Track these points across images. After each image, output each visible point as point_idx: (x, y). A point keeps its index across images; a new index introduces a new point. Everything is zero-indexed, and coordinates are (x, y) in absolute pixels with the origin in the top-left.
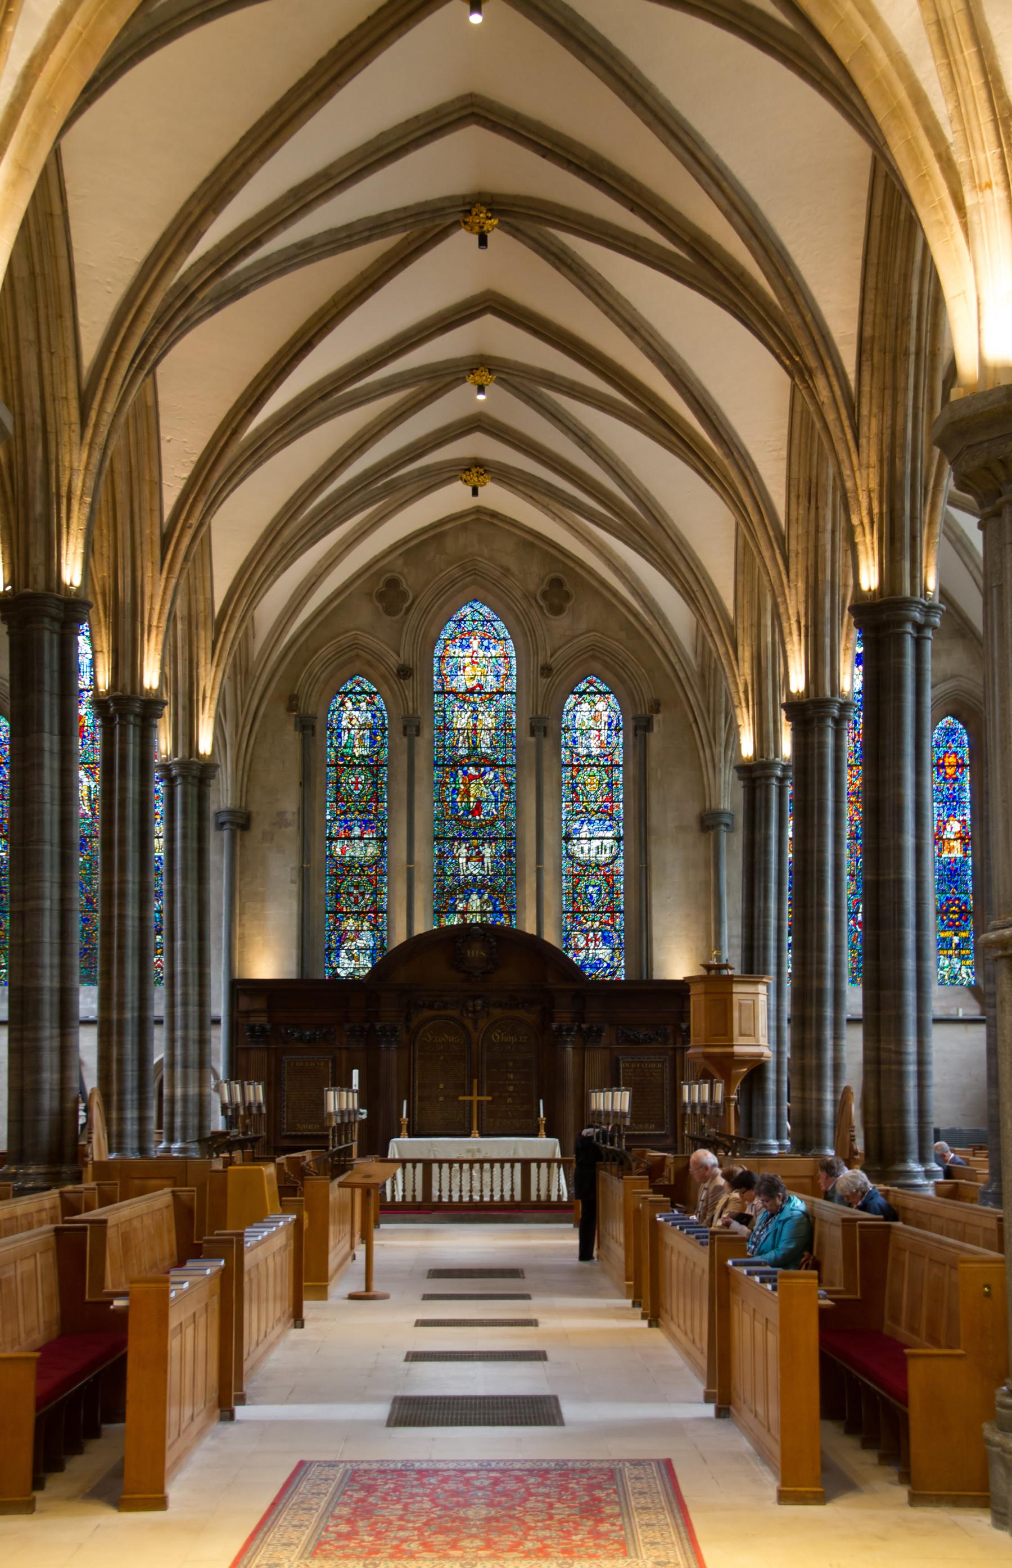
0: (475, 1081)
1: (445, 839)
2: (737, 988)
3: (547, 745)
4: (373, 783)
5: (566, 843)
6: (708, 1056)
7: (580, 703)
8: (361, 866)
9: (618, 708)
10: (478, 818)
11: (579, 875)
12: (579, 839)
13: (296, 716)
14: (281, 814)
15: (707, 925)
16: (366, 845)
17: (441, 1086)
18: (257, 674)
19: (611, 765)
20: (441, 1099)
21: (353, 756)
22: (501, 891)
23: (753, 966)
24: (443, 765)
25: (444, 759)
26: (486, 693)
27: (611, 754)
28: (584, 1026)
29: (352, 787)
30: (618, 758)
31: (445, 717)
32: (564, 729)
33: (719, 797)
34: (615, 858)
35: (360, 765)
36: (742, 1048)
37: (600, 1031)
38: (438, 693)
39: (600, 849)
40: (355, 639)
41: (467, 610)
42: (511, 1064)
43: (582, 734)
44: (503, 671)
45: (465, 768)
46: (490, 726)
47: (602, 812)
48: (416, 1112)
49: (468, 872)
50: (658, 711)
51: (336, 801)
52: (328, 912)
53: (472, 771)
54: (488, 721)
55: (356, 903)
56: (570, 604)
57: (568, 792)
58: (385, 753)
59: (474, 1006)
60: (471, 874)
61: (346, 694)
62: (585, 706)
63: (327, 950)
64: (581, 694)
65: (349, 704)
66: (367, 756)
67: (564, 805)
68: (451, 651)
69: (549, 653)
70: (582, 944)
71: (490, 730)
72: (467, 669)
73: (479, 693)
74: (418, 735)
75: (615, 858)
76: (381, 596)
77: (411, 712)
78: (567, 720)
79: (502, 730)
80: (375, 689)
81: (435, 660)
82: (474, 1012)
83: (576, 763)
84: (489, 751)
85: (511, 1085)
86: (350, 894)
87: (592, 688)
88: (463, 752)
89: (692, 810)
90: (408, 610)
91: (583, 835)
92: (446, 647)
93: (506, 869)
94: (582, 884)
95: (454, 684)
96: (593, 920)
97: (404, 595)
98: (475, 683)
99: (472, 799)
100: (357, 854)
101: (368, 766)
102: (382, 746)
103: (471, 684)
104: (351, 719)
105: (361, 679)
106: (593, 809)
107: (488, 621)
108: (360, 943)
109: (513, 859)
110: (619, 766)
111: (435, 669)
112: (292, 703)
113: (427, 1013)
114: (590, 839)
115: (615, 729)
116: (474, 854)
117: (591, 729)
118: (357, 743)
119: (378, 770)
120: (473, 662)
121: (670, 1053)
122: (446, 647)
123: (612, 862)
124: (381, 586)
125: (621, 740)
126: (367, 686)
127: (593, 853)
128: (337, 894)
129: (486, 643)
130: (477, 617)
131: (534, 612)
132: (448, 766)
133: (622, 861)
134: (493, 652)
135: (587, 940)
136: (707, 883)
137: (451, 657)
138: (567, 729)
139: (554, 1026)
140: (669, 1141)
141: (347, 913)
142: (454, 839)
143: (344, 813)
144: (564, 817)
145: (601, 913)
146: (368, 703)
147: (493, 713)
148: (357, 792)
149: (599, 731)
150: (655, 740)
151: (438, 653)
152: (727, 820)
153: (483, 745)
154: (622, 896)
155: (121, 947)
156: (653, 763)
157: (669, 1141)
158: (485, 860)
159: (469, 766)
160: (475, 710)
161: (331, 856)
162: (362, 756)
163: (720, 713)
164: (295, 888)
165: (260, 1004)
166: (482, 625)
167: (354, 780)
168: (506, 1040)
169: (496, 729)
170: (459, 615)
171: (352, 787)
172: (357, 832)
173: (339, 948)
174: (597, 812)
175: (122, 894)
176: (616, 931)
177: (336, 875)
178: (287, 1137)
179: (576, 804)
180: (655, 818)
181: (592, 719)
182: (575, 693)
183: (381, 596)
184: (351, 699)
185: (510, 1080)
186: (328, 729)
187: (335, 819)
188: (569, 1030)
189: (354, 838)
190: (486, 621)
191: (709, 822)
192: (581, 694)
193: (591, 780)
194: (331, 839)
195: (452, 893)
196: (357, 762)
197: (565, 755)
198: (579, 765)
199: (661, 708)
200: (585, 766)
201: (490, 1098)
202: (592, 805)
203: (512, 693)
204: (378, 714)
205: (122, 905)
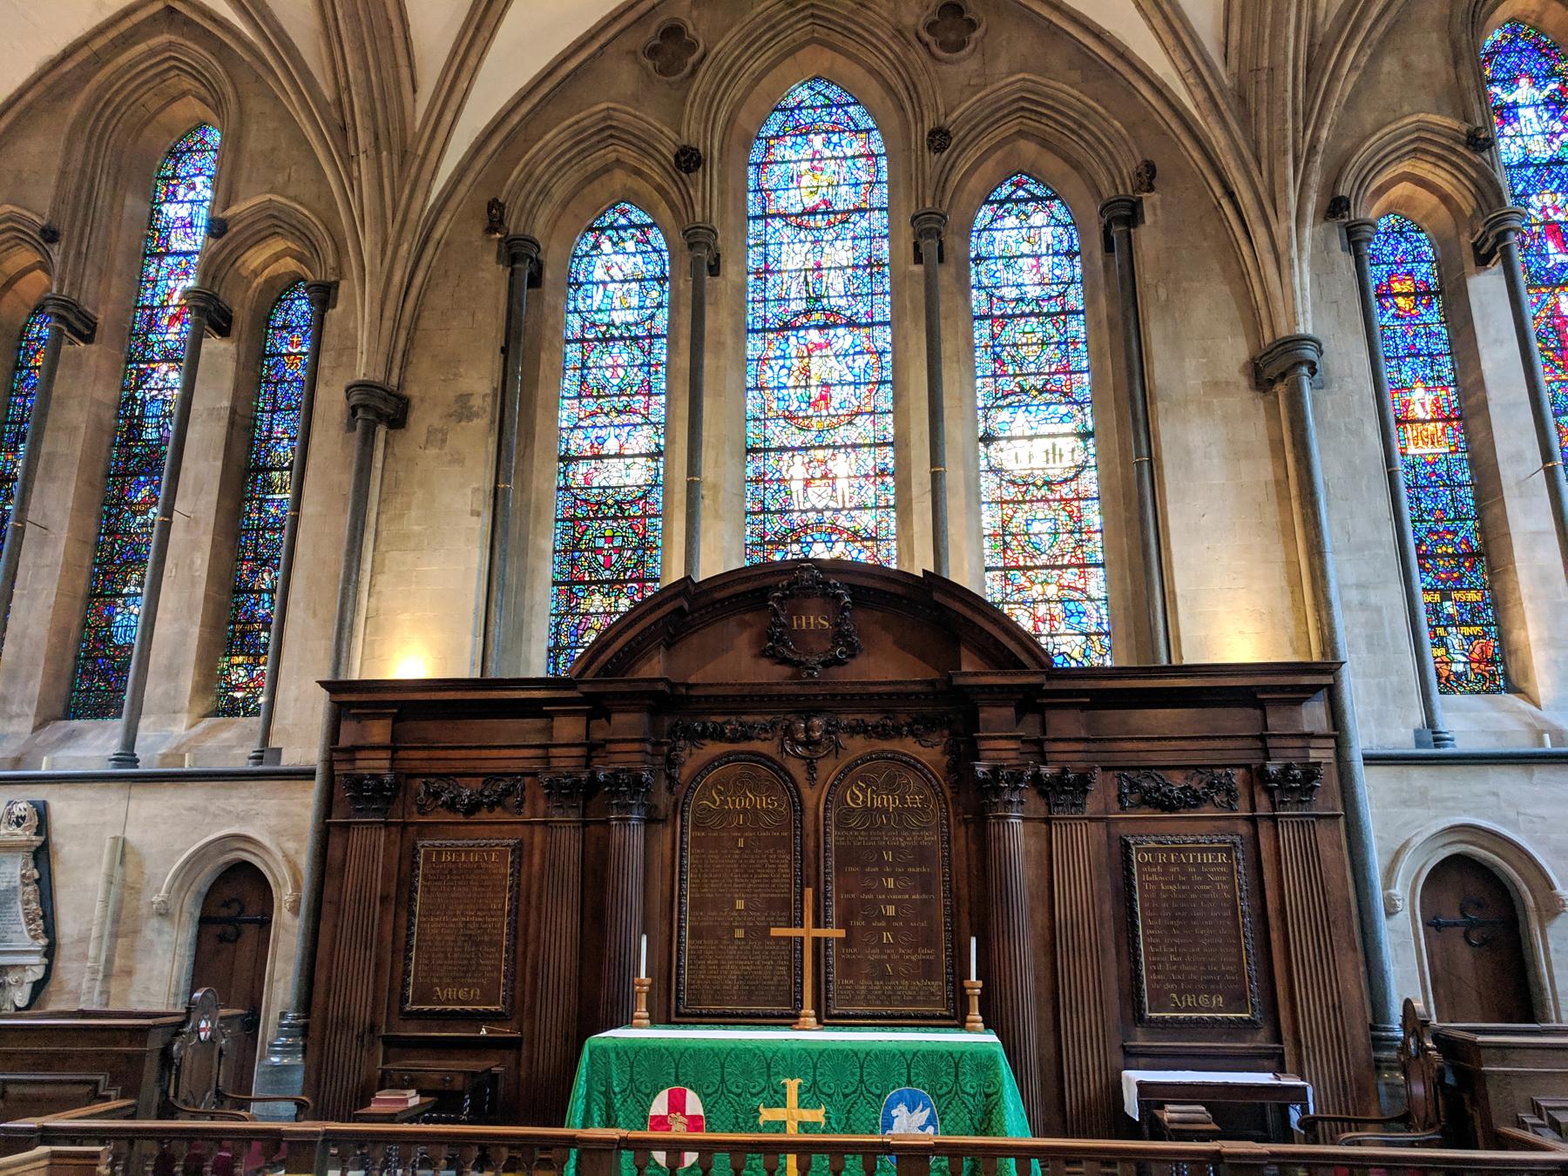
0: (809, 892)
1: (770, 450)
3: (945, 276)
4: (642, 365)
5: (987, 446)
7: (1002, 217)
8: (617, 502)
9: (1069, 220)
10: (824, 413)
11: (1013, 501)
12: (1010, 439)
13: (500, 240)
14: (464, 398)
15: (1291, 565)
16: (628, 467)
17: (740, 905)
18: (420, 152)
19: (1063, 312)
20: (740, 933)
21: (611, 324)
22: (866, 539)
24: (764, 330)
25: (765, 320)
26: (835, 213)
27: (1062, 294)
28: (1046, 771)
29: (608, 374)
30: (1075, 299)
31: (766, 256)
32: (974, 260)
33: (1294, 314)
34: (1082, 468)
35: (622, 338)
37: (1083, 781)
38: (755, 218)
39: (1054, 453)
40: (604, 119)
42: (888, 856)
43: (1007, 266)
45: (802, 333)
46: (845, 263)
47: (1051, 392)
48: (685, 961)
49: (808, 505)
50: (1151, 189)
51: (579, 396)
52: (555, 583)
53: (814, 336)
54: (840, 253)
55: (608, 565)
56: (977, 34)
57: (987, 358)
58: (662, 317)
59: (807, 730)
60: (814, 509)
61: (603, 230)
62: (1010, 221)
63: (549, 650)
64: (1002, 203)
65: (607, 247)
66: (636, 324)
67: (979, 382)
68: (780, 152)
69: (942, 111)
71: (842, 268)
72: (805, 181)
73: (823, 214)
74: (715, 270)
75: (1082, 468)
76: (653, 52)
77: (699, 219)
78: (978, 245)
79: (865, 267)
80: (649, 221)
81: (751, 170)
82: (809, 743)
83: (997, 313)
84: (843, 302)
85: (891, 902)
86: (599, 550)
87: (1021, 193)
89: (1235, 351)
90: (694, 72)
91: (1017, 432)
92: (768, 149)
93: (877, 497)
94: (1020, 518)
95: (783, 203)
96: (1045, 582)
97: (692, 46)
98: (817, 199)
99: (813, 382)
100: (613, 483)
101: (635, 339)
102: (660, 306)
103: (810, 202)
104: (608, 269)
105: (627, 206)
106: (1033, 387)
107: (839, 106)
109: (889, 480)
110: (1078, 313)
111: (751, 183)
112: (495, 215)
113: (714, 749)
114: (1030, 438)
115: (1067, 254)
116: (818, 475)
117: (1022, 256)
118: (617, 304)
119: (651, 344)
120: (814, 168)
121: (1244, 829)
122: (768, 149)
123: (1076, 476)
124: (650, 33)
125: (1078, 271)
126: (638, 216)
127: (1039, 461)
128: (572, 549)
129: (835, 138)
130: (820, 100)
131: (918, 57)
132: (770, 330)
133: (1094, 474)
134: (849, 152)
135: (1034, 617)
136: (1281, 484)
137: (776, 162)
138: (979, 259)
140: (1261, 1040)
141: (591, 583)
142: (782, 449)
143: (593, 414)
144: (980, 404)
145: (1061, 567)
146: (638, 242)
147: (849, 243)
148: (615, 381)
149: (1037, 257)
150: (1148, 239)
151: (755, 157)
152: (1311, 354)
153: (832, 293)
154: (1098, 536)
156: (1146, 275)
157: (1261, 1040)
158: (841, 484)
159: (807, 329)
160: (816, 242)
161: (567, 488)
162: (627, 325)
163: (1285, 153)
164: (482, 525)
165: (379, 731)
166: (830, 114)
167: (610, 361)
169: (855, 267)
171: (608, 374)
172: (611, 446)
174: (1041, 392)
176: (1089, 599)
177: (574, 519)
178: (418, 1015)
179: (1001, 380)
180: (1161, 369)
181: (1025, 248)
182: (992, 203)
183: (653, 52)
184: (610, 239)
186: (570, 285)
187: (576, 427)
188: (1015, 778)
189: (608, 456)
191: (1279, 368)
192: (1002, 203)
194: (567, 459)
196: (616, 334)
197: (978, 302)
198: (1003, 316)
199: (1155, 183)
200: (1013, 316)
201: (842, 933)
202: (1032, 380)
203: (881, 209)
204: (655, 256)
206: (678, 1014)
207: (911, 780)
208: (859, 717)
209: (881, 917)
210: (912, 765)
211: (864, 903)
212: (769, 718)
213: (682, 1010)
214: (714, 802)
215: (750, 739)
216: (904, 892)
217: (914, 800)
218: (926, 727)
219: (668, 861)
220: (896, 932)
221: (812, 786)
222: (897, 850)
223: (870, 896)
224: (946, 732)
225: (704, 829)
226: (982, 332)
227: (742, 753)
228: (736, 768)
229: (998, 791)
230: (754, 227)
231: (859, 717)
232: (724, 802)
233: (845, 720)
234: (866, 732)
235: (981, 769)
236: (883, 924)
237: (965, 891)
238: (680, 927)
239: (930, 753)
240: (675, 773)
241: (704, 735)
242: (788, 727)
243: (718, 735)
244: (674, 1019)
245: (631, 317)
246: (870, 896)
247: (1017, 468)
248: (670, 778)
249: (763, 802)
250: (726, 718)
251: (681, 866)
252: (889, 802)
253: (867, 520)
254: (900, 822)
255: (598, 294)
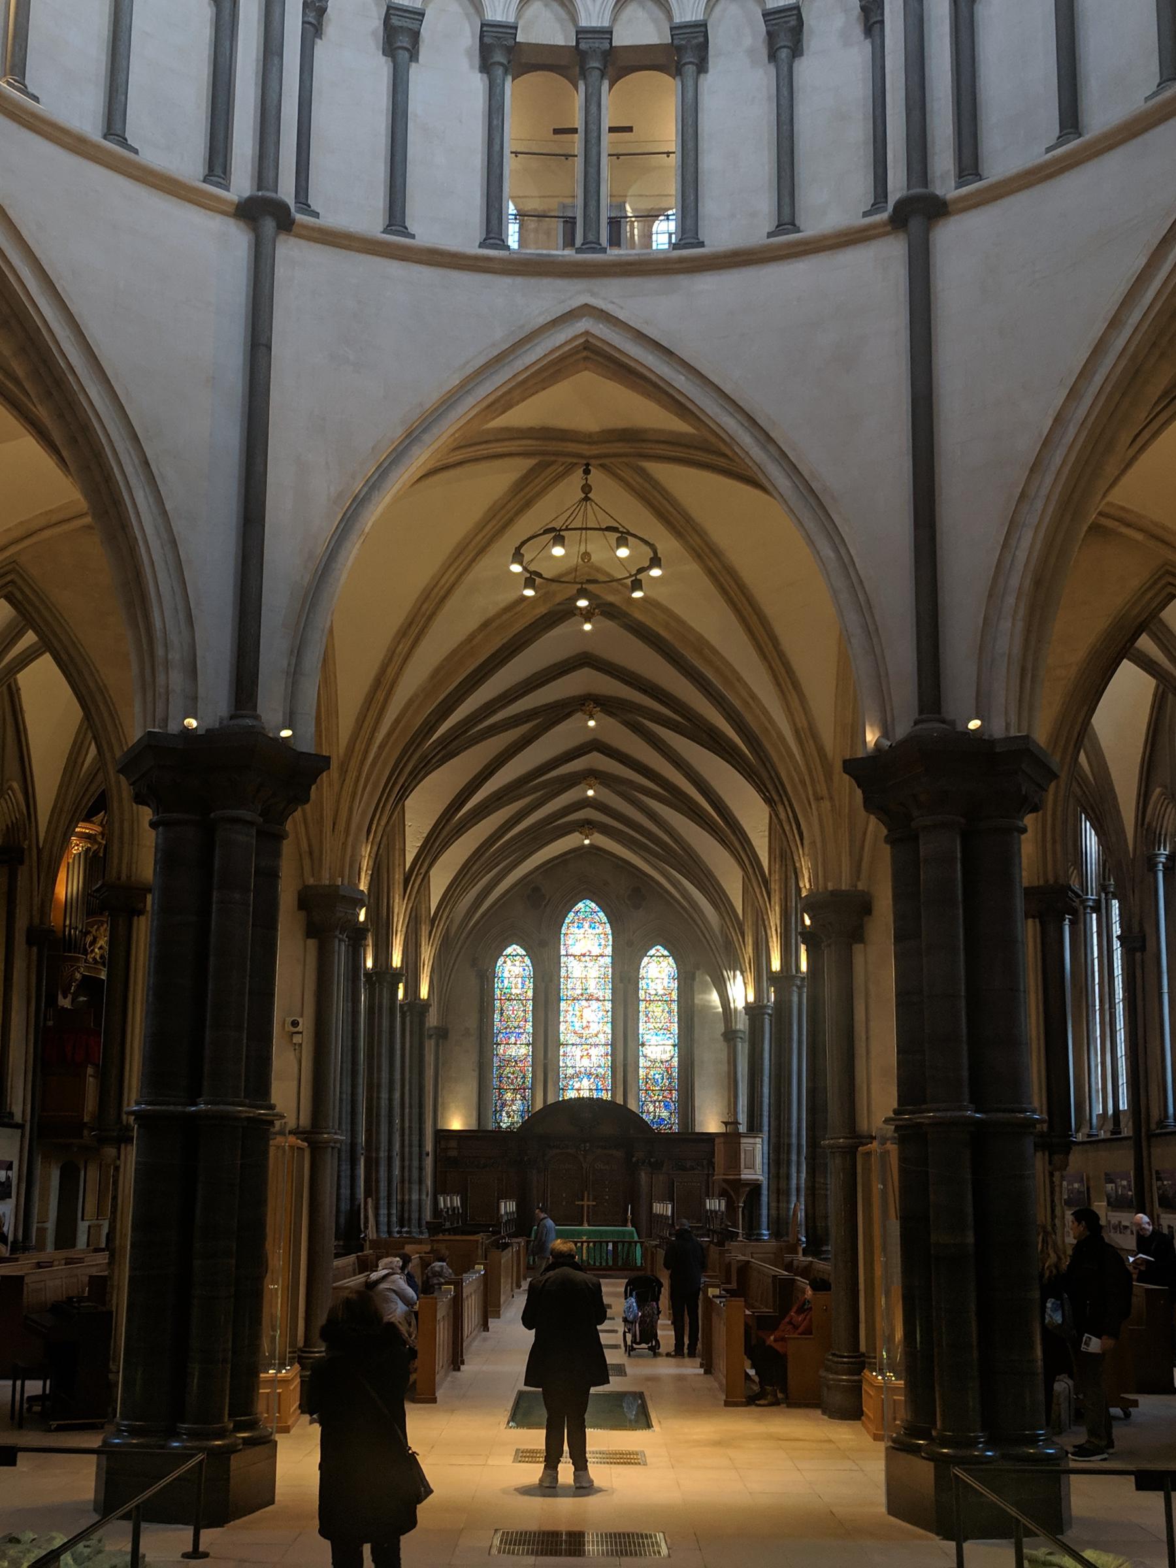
2: (743, 1140)
6: (725, 1181)
23: (754, 1128)
30: (675, 996)
36: (746, 1175)
41: (580, 905)
44: (603, 942)
53: (584, 1003)
58: (530, 994)
65: (509, 962)
68: (572, 930)
70: (651, 1109)
78: (642, 972)
88: (579, 992)
108: (514, 1108)
134: (597, 931)
136: (729, 1073)
139: (634, 1159)
155: (378, 1115)
164: (476, 1074)
170: (576, 908)
172: (513, 1040)
173: (501, 1111)
175: (379, 1086)
190: (593, 912)
193: (657, 1010)
195: (572, 1077)
205: (379, 1092)
226: (642, 1005)
230: (563, 959)
245: (518, 991)
247: (653, 1057)
253: (600, 1070)
255: (506, 981)
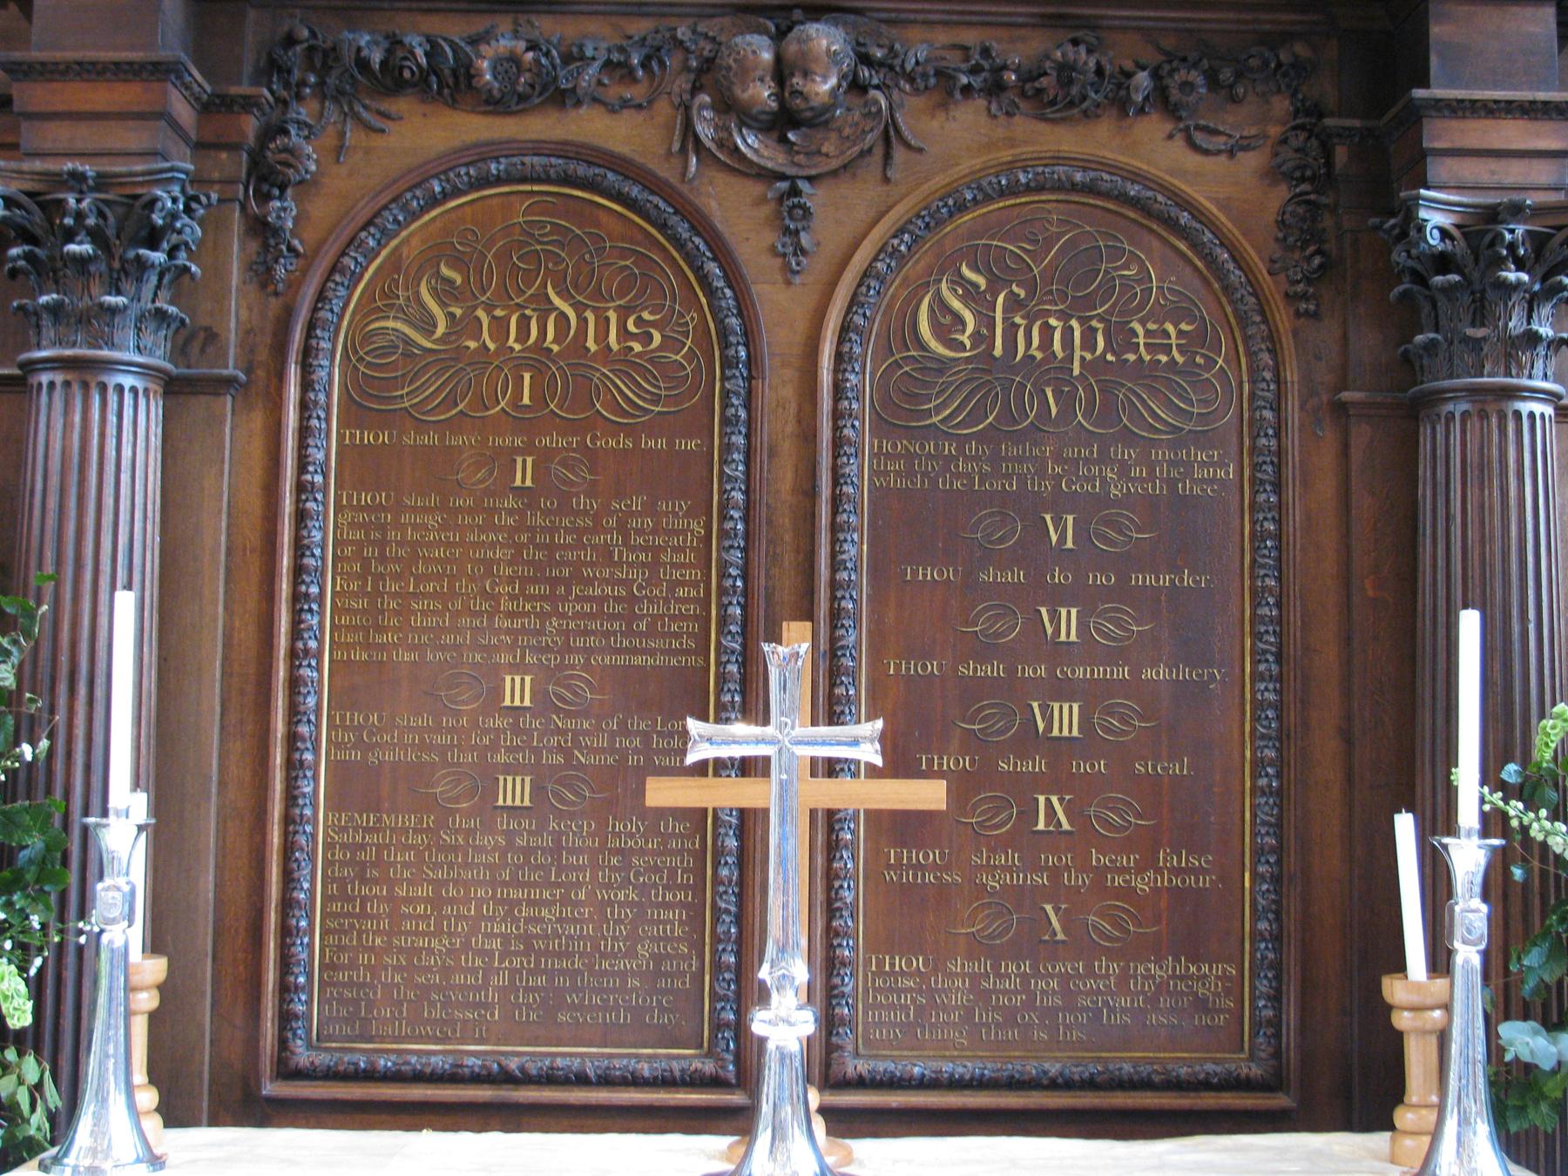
17: (518, 690)
20: (515, 791)
42: (1063, 532)
48: (313, 885)
59: (781, 72)
85: (1062, 690)
113: (425, 132)
168: (1028, 345)
185: (1058, 652)
206: (287, 1071)
207: (1152, 269)
208: (970, 37)
209: (1029, 740)
210: (1160, 213)
211: (973, 691)
212: (640, 27)
213: (303, 1056)
214: (428, 326)
215: (562, 98)
216: (1113, 656)
217: (1158, 338)
218: (1213, 81)
219: (252, 535)
220: (1080, 793)
221: (789, 273)
222: (1093, 509)
223: (994, 670)
224: (1281, 105)
225: (384, 420)
227: (538, 148)
228: (517, 206)
229: (1484, 299)
231: (970, 37)
232: (464, 326)
233: (918, 49)
234: (995, 88)
235: (1436, 219)
236: (1038, 765)
237: (1328, 658)
238: (293, 767)
239: (1222, 174)
240: (283, 210)
241: (392, 79)
242: (709, 64)
243: (451, 83)
244: (270, 1088)
246: (994, 670)
248: (261, 228)
249: (609, 331)
250: (479, 24)
251: (300, 548)
252: (1068, 339)
254: (1108, 414)
